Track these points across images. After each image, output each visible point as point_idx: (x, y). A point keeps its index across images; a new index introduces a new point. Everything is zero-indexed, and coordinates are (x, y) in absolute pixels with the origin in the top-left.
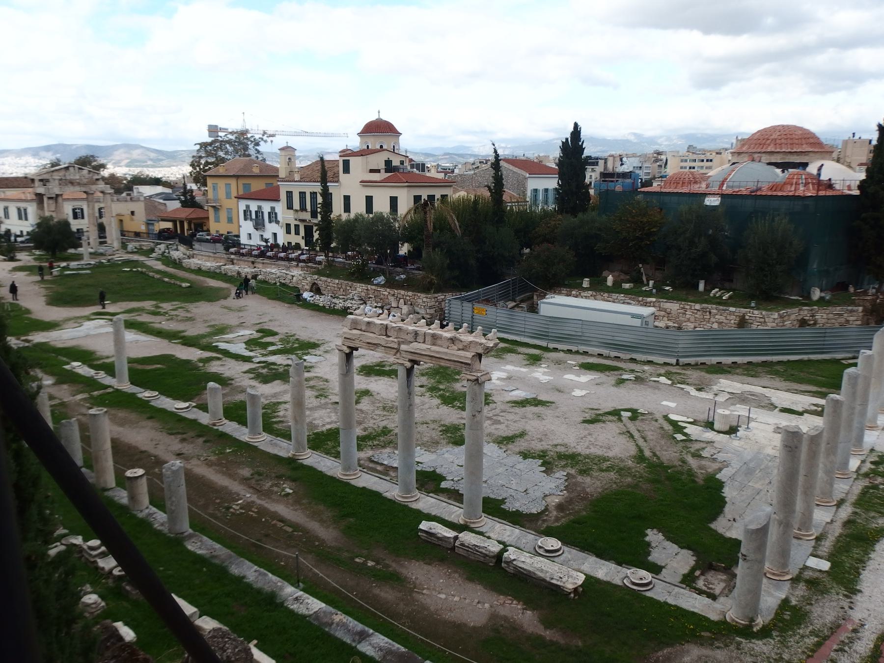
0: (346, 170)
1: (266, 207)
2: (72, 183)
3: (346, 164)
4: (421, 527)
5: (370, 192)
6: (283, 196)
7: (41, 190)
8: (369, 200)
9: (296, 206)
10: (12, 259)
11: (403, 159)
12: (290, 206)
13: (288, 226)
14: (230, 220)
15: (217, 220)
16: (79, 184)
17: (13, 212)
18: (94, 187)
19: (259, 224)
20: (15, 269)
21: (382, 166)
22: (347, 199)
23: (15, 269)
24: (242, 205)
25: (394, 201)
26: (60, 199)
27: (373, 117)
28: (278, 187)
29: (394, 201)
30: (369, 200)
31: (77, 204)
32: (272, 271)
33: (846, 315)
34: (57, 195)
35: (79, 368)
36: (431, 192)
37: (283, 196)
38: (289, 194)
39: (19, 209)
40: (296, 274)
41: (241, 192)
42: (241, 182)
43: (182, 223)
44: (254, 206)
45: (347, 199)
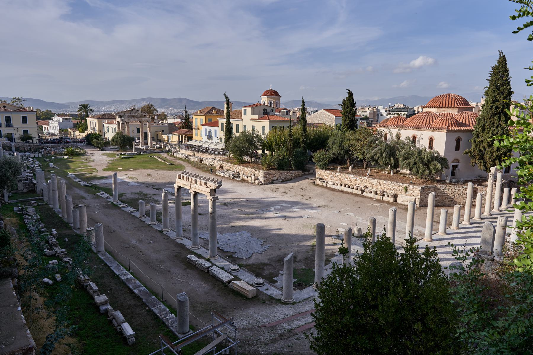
0: (245, 114)
1: (213, 129)
2: (133, 117)
3: (245, 110)
4: (188, 257)
6: (220, 125)
8: (254, 127)
9: (224, 130)
10: (103, 150)
11: (272, 109)
12: (222, 130)
14: (201, 136)
15: (197, 135)
16: (137, 118)
18: (143, 119)
19: (210, 137)
20: (103, 154)
21: (262, 112)
22: (245, 127)
23: (103, 154)
25: (264, 128)
28: (217, 122)
29: (264, 128)
30: (254, 127)
32: (208, 159)
35: (102, 194)
38: (222, 124)
40: (216, 161)
41: (204, 123)
42: (208, 117)
44: (208, 128)
45: (245, 127)
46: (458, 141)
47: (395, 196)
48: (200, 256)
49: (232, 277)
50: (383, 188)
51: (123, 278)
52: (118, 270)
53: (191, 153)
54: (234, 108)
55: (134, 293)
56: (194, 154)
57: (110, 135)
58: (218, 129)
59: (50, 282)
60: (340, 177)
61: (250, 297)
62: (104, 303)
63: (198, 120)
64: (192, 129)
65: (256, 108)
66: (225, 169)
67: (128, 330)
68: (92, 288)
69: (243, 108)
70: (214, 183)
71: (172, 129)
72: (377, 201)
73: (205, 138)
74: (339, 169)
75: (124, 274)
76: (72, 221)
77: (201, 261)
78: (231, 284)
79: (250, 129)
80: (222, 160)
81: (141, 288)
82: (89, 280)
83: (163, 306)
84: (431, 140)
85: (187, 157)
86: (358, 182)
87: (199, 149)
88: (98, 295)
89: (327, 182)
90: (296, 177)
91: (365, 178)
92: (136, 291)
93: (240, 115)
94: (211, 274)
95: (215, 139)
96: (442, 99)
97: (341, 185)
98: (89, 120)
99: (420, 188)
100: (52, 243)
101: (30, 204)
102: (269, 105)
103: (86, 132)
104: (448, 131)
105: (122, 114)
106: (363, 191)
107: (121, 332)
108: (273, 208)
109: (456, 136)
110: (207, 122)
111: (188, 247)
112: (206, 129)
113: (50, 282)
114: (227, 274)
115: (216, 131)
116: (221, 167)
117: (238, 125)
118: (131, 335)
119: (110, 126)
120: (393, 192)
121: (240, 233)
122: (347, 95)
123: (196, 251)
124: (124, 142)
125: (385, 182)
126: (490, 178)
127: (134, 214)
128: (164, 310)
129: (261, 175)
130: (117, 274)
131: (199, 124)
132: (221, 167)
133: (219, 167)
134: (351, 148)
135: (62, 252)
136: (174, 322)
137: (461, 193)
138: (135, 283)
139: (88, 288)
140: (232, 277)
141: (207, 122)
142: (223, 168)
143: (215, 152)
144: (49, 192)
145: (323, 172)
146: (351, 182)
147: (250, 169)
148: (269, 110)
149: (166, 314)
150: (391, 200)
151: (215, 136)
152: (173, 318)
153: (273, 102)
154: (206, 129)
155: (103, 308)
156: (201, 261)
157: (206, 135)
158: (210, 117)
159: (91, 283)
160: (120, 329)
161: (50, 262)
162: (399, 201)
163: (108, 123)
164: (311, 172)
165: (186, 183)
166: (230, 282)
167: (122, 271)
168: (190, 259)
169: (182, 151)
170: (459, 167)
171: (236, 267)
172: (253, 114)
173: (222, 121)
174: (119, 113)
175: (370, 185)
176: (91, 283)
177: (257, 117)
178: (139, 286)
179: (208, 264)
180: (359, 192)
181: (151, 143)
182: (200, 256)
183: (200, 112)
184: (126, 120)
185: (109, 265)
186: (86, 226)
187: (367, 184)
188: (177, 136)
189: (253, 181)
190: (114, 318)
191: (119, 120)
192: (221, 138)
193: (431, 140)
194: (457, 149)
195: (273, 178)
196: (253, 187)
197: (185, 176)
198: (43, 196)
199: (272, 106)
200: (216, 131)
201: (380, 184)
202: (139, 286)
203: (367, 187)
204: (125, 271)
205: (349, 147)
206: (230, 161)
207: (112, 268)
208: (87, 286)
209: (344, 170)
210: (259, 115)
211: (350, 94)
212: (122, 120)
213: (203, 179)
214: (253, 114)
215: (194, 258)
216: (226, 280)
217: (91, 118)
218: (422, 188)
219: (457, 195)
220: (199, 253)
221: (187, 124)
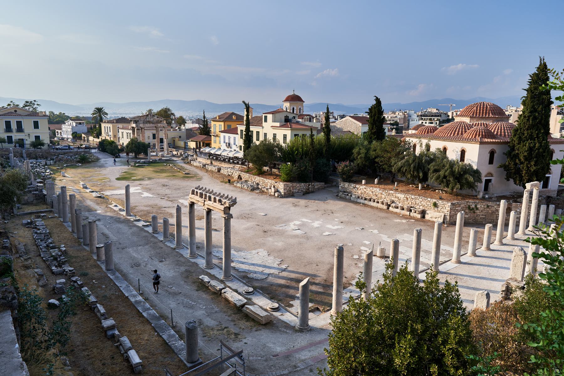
0: (266, 121)
1: (232, 136)
2: (149, 122)
3: (266, 117)
4: (200, 277)
5: (275, 131)
6: (239, 132)
7: (134, 125)
8: (275, 136)
11: (294, 115)
12: (242, 138)
13: (241, 146)
14: (220, 143)
15: (215, 142)
16: (153, 123)
17: (125, 135)
18: (159, 125)
19: (229, 145)
21: (283, 119)
22: (265, 135)
24: (222, 135)
25: (285, 137)
26: (143, 130)
27: (292, 93)
28: (237, 128)
29: (285, 137)
31: (154, 132)
33: (496, 207)
34: (142, 128)
36: (304, 132)
37: (239, 132)
39: (127, 133)
41: (223, 129)
42: (227, 123)
43: (200, 142)
44: (227, 135)
45: (265, 135)
46: (492, 153)
47: (423, 213)
48: (213, 277)
49: (246, 301)
50: (410, 203)
51: (133, 300)
52: (127, 291)
53: (209, 162)
54: (254, 114)
55: (143, 316)
56: (212, 163)
57: (124, 141)
58: (238, 137)
59: (56, 302)
60: (365, 190)
61: (264, 322)
62: (112, 327)
63: (216, 127)
64: (211, 136)
65: (277, 115)
66: (243, 180)
67: (135, 358)
68: (99, 311)
69: (264, 115)
70: (229, 200)
71: (190, 134)
72: (404, 217)
73: (224, 146)
74: (363, 182)
75: (134, 296)
76: (82, 236)
77: (213, 283)
78: (244, 309)
79: (270, 137)
80: (241, 171)
81: (150, 311)
82: (96, 302)
83: (172, 332)
84: (463, 152)
85: (205, 165)
86: (383, 196)
87: (216, 157)
88: (106, 319)
89: (351, 196)
90: (319, 189)
91: (391, 192)
92: (145, 314)
93: (260, 122)
94: (223, 296)
95: (234, 147)
96: (475, 108)
97: (366, 199)
98: (103, 125)
99: (450, 204)
100: (60, 261)
101: (39, 217)
102: (292, 112)
103: (100, 137)
104: (481, 143)
105: (137, 119)
106: (389, 206)
107: (128, 360)
108: (293, 223)
109: (489, 148)
110: (226, 129)
111: (201, 266)
112: (224, 136)
113: (56, 302)
114: (241, 297)
115: (235, 138)
116: (240, 177)
117: (258, 133)
118: (137, 363)
119: (125, 131)
120: (421, 207)
121: (256, 251)
122: (374, 102)
123: (209, 271)
124: (138, 149)
125: (413, 197)
126: (526, 195)
127: (146, 229)
128: (173, 336)
129: (281, 186)
130: (127, 295)
131: (218, 130)
132: (240, 177)
133: (237, 177)
134: (377, 160)
135: (70, 271)
136: (183, 350)
137: (494, 209)
138: (144, 306)
139: (96, 310)
140: (246, 301)
141: (226, 129)
142: (241, 179)
143: (233, 160)
144: (59, 205)
145: (347, 185)
146: (376, 196)
147: (270, 181)
148: (291, 116)
149: (176, 340)
150: (419, 216)
151: (235, 144)
152: (182, 345)
153: (295, 108)
154: (224, 136)
155: (110, 333)
156: (213, 283)
157: (224, 142)
158: (229, 123)
159: (98, 305)
160: (127, 357)
161: (58, 281)
162: (427, 217)
163: (122, 129)
164: (334, 184)
165: (200, 199)
166: (243, 306)
167: (131, 292)
168: (202, 280)
169: (199, 159)
170: (493, 182)
171: (251, 289)
172: (274, 121)
173: (242, 128)
174: (134, 118)
175: (397, 199)
176: (98, 305)
177: (278, 124)
178: (149, 309)
179: (219, 286)
180: (385, 207)
181: (168, 150)
182: (213, 277)
183: (219, 118)
184: (141, 125)
185: (119, 285)
186: (96, 242)
187: (393, 199)
188: (195, 143)
189: (273, 194)
190: (121, 344)
191: (134, 125)
192: (241, 146)
193: (463, 152)
194: (491, 162)
195: (294, 191)
196: (273, 200)
197: (199, 192)
198: (52, 207)
199: (295, 112)
200: (235, 138)
201: (407, 199)
202: (149, 309)
203: (393, 202)
204: (135, 292)
205: (376, 158)
206: (248, 171)
207: (121, 289)
208: (94, 308)
209: (370, 182)
210: (280, 122)
211: (378, 101)
212: (137, 126)
213: (218, 196)
214: (274, 121)
215: (206, 279)
216: (239, 304)
217: (105, 122)
218: (452, 204)
219: (490, 212)
220: (212, 274)
221: (205, 130)
